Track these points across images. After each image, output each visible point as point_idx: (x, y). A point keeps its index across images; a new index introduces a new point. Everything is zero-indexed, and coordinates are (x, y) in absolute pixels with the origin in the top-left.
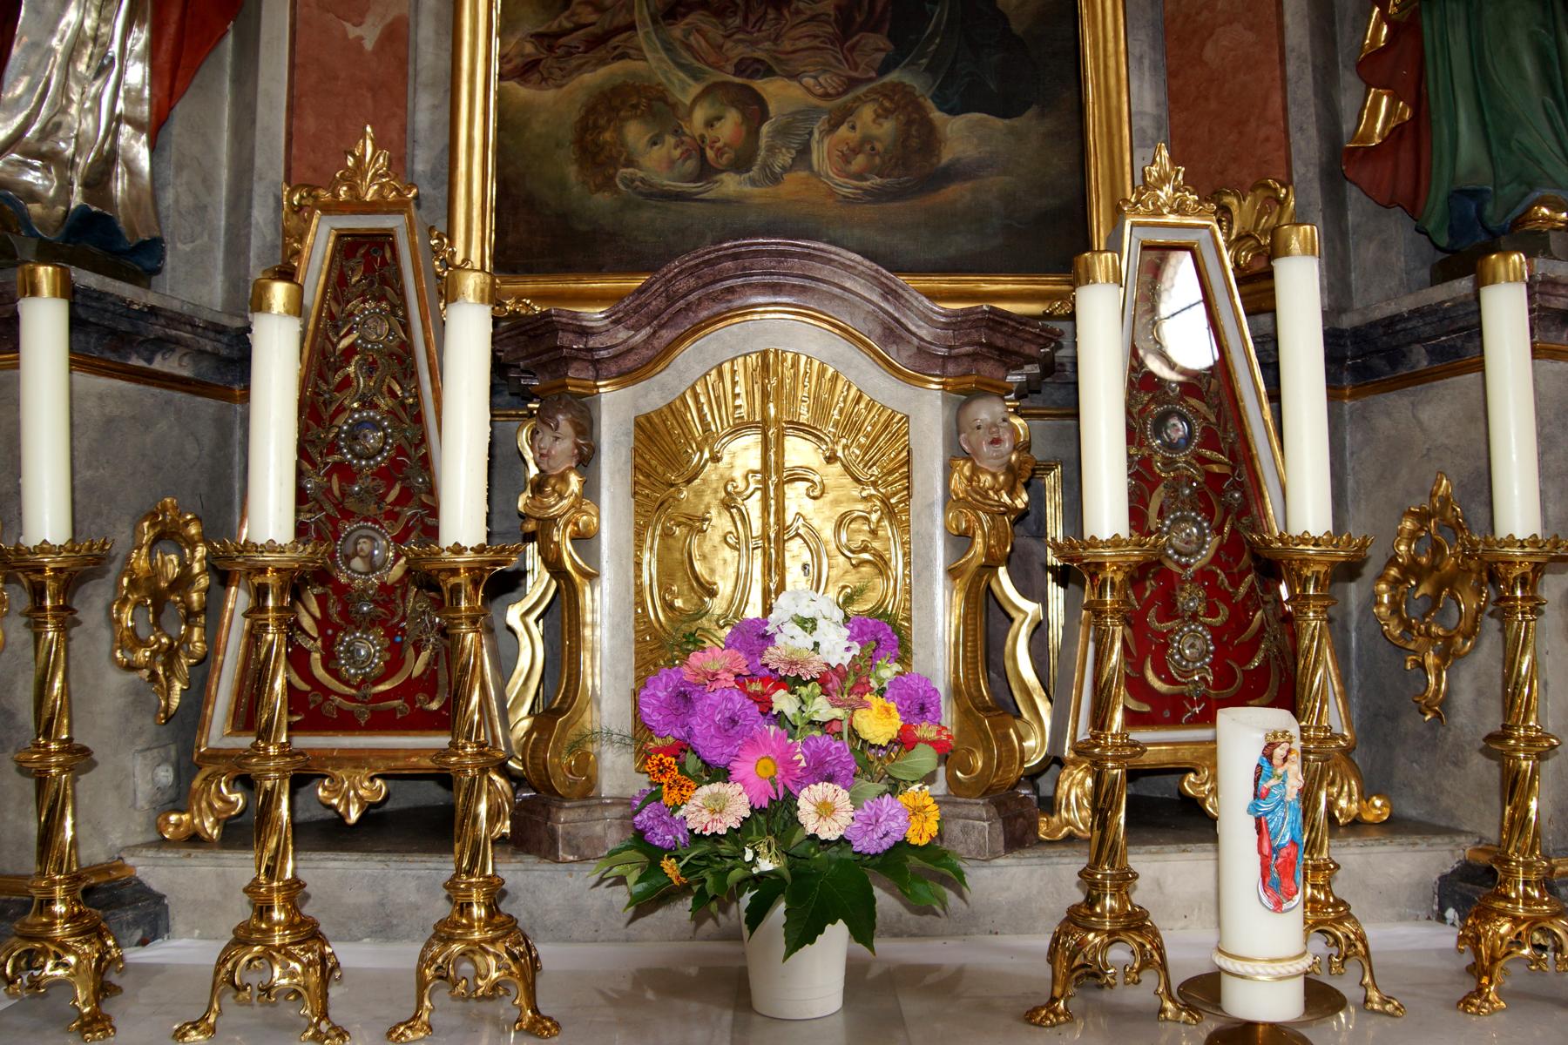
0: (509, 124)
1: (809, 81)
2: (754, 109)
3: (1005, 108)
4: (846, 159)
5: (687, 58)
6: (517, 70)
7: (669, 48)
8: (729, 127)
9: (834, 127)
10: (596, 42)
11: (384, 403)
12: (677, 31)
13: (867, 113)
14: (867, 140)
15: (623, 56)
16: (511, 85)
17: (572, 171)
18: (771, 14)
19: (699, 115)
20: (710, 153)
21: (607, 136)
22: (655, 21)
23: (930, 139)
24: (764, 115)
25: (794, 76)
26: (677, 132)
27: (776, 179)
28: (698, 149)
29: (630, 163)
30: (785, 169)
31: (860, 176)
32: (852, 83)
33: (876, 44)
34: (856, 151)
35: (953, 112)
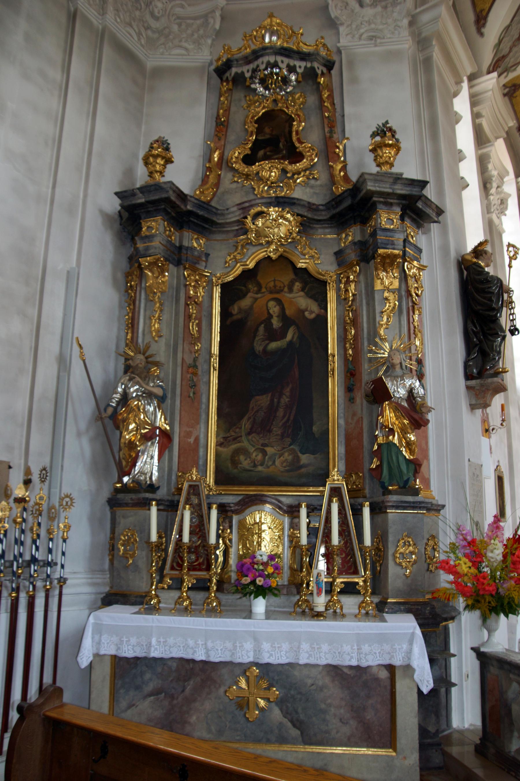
0: (218, 455)
1: (275, 448)
2: (265, 453)
3: (313, 453)
4: (282, 464)
5: (252, 443)
6: (219, 444)
7: (248, 441)
8: (260, 457)
9: (280, 457)
10: (234, 439)
11: (196, 514)
12: (250, 437)
13: (286, 454)
14: (286, 460)
15: (240, 442)
16: (218, 447)
17: (230, 465)
18: (268, 434)
19: (254, 454)
20: (256, 462)
21: (237, 458)
22: (246, 435)
23: (298, 459)
24: (266, 455)
25: (272, 447)
26: (250, 458)
27: (268, 467)
28: (254, 461)
29: (241, 464)
30: (271, 466)
31: (285, 467)
32: (284, 448)
33: (288, 440)
34: (284, 462)
35: (303, 454)
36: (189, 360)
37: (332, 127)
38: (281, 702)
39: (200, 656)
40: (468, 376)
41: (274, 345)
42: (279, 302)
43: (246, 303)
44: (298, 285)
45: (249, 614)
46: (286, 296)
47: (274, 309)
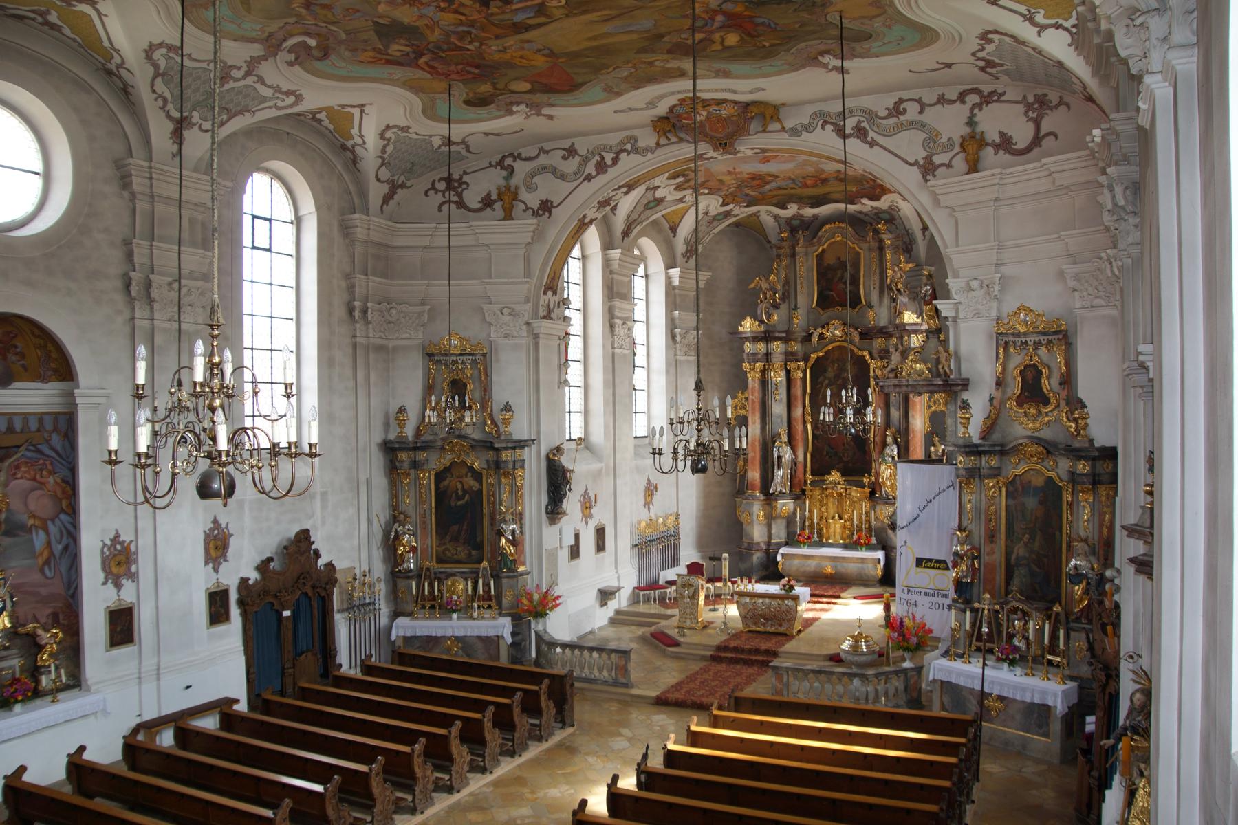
0: (437, 551)
23: (470, 553)
36: (422, 512)
37: (485, 390)
38: (462, 648)
39: (434, 635)
40: (547, 513)
41: (459, 503)
42: (461, 482)
43: (446, 483)
44: (469, 474)
45: (451, 619)
46: (465, 480)
47: (459, 486)
